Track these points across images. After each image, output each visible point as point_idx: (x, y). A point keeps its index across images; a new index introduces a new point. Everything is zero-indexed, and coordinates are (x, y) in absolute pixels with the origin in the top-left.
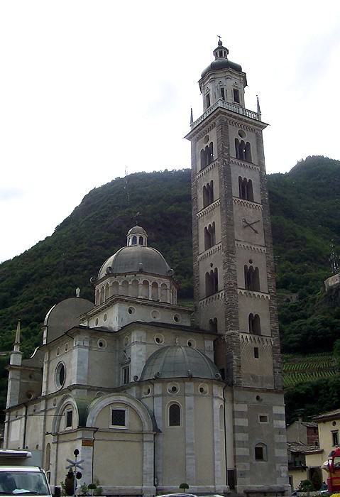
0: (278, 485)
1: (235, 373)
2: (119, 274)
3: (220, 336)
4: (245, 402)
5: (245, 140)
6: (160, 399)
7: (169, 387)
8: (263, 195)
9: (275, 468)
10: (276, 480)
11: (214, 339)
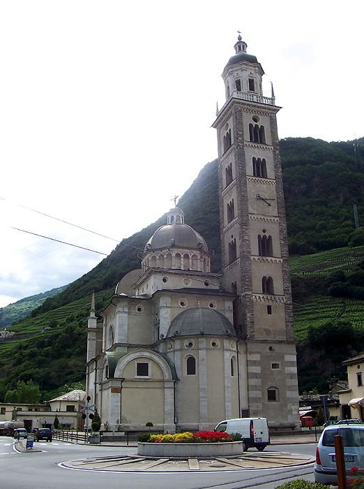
0: (289, 421)
1: (248, 328)
2: (156, 250)
3: (239, 296)
4: (258, 353)
6: (179, 352)
7: (186, 343)
8: (276, 172)
9: (287, 408)
10: (287, 417)
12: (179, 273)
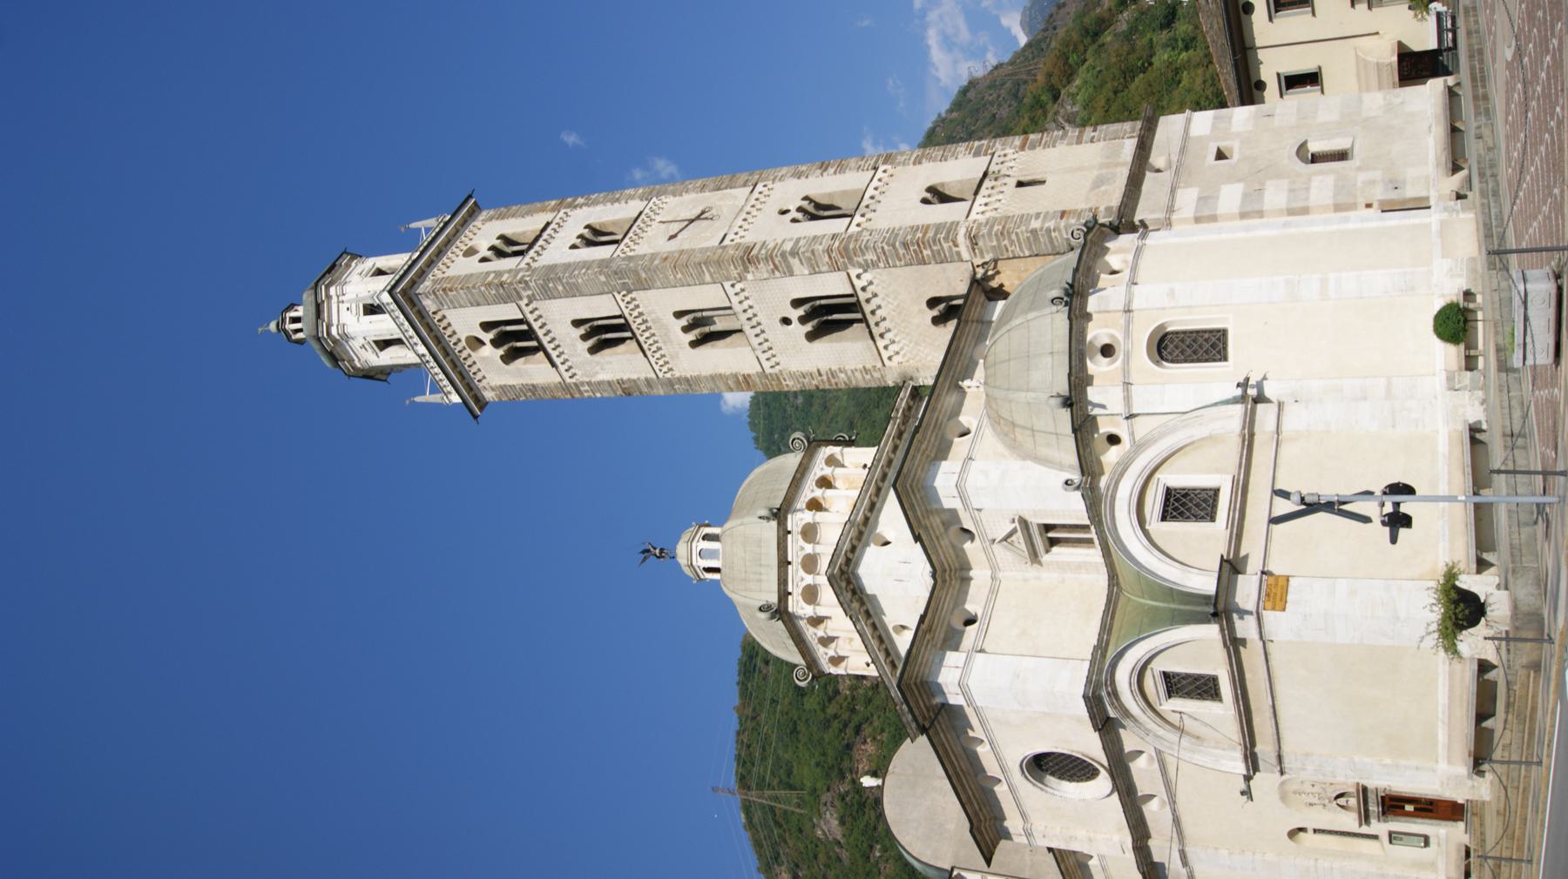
2: (783, 581)
3: (975, 282)
11: (983, 298)
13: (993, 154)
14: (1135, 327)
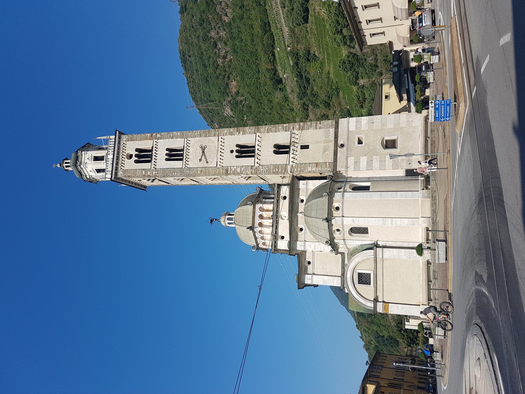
5: (134, 153)
12: (275, 225)
13: (291, 131)
14: (345, 228)
